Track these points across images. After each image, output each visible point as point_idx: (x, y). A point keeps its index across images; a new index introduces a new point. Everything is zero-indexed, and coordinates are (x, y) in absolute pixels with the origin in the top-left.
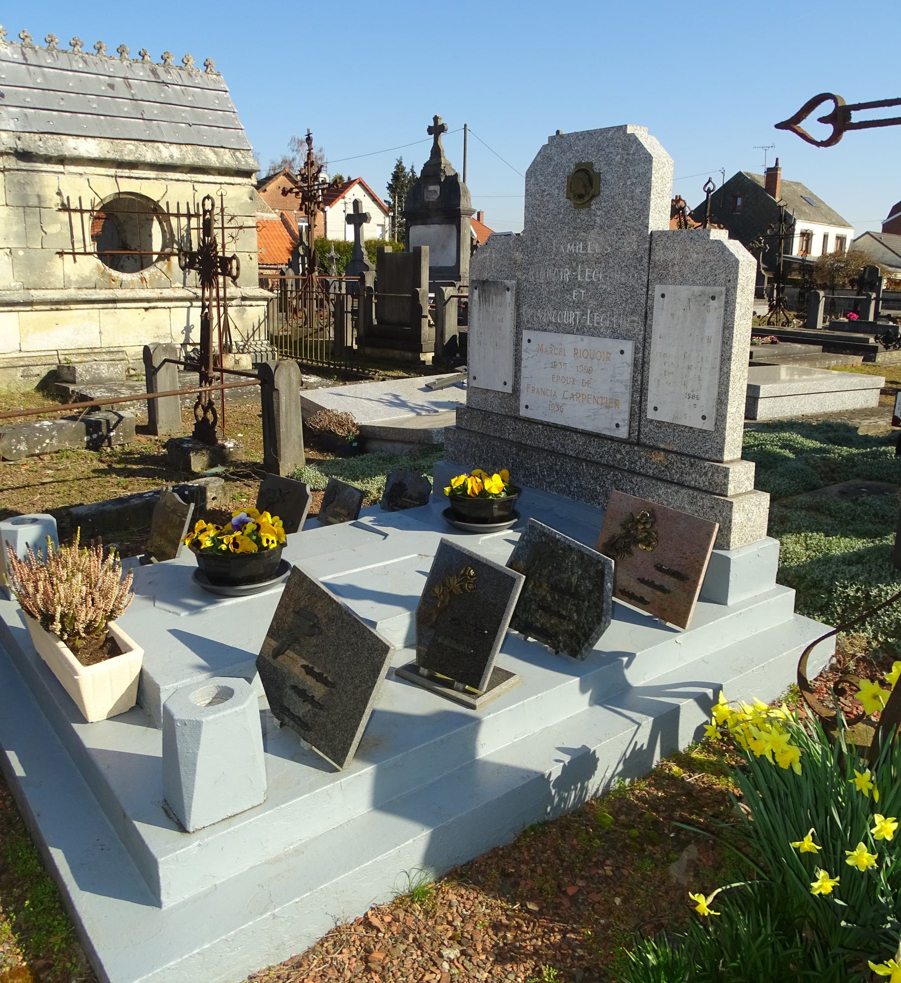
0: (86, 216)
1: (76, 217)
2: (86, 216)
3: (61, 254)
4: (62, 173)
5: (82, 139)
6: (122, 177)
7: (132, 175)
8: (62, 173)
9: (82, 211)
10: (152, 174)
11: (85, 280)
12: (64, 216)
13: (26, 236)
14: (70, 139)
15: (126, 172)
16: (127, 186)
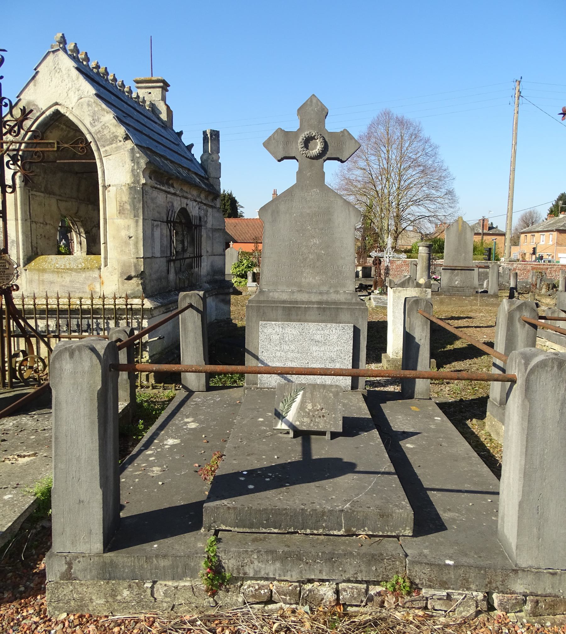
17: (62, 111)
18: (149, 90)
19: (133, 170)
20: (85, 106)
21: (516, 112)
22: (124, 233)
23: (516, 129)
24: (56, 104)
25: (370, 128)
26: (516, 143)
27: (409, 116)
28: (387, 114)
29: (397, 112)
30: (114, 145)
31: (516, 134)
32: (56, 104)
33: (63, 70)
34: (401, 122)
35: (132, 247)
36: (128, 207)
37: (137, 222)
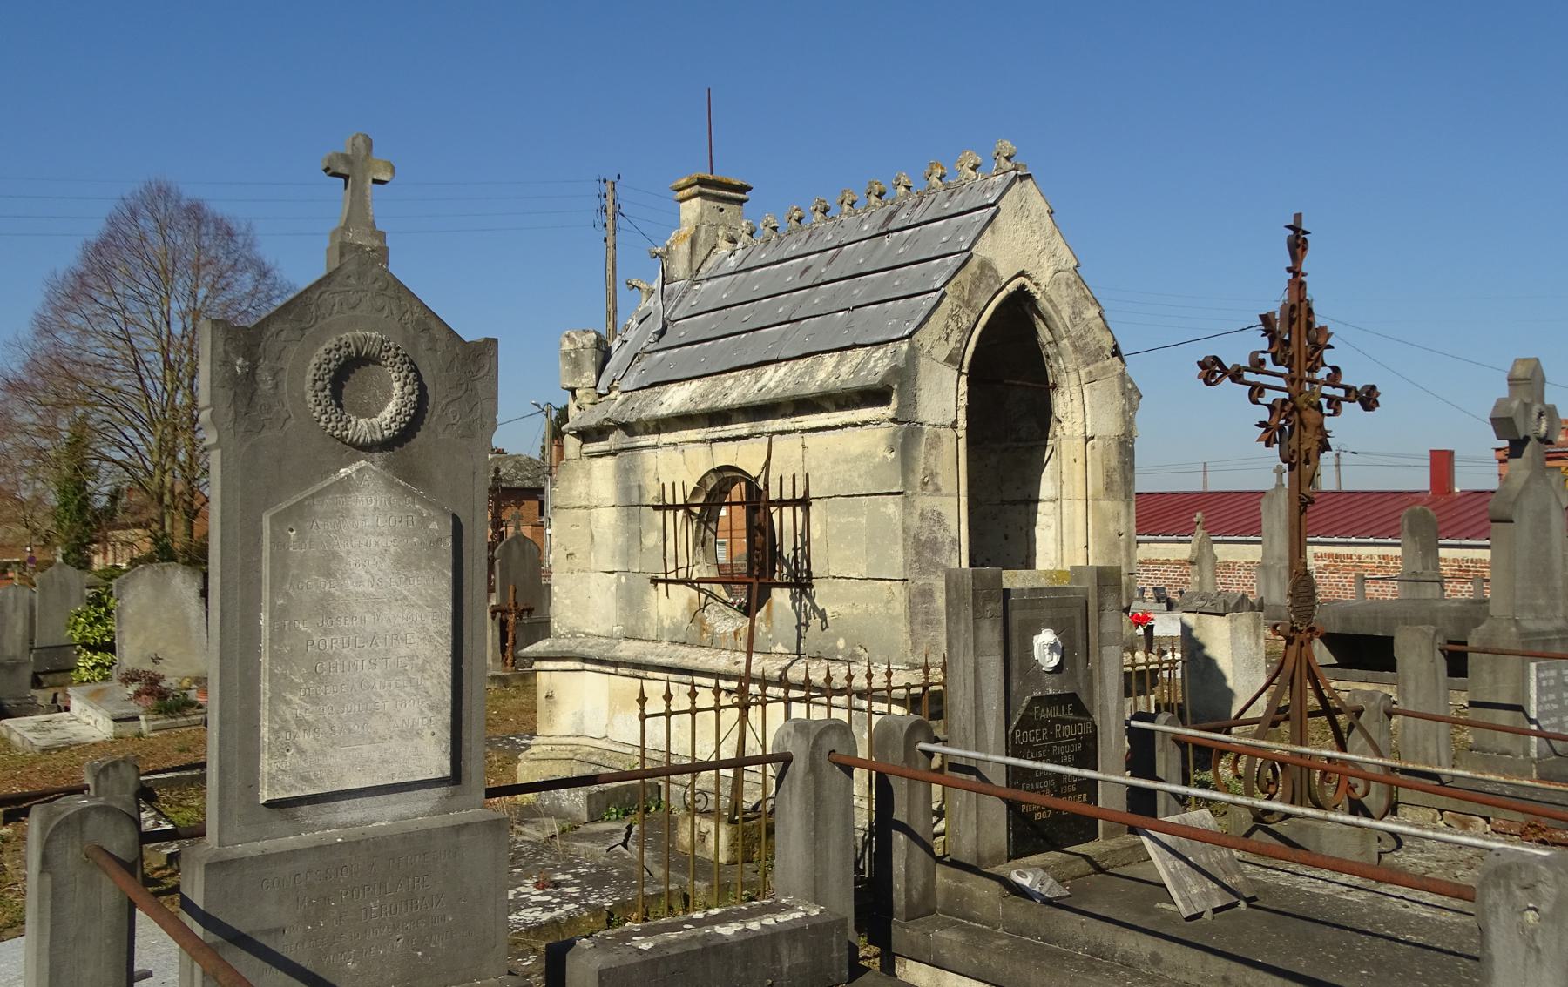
0: (680, 513)
1: (670, 514)
2: (680, 513)
3: (655, 581)
4: (656, 446)
5: (687, 384)
6: (713, 441)
7: (723, 435)
8: (656, 446)
9: (675, 507)
10: (743, 428)
11: (676, 629)
12: (659, 514)
13: (627, 554)
14: (674, 388)
15: (718, 432)
16: (726, 455)
17: (1031, 288)
18: (721, 205)
19: (1124, 411)
20: (1063, 287)
21: (610, 243)
22: (1112, 528)
23: (614, 279)
24: (1022, 274)
25: (112, 221)
26: (615, 311)
27: (220, 205)
28: (164, 192)
29: (190, 192)
30: (1100, 364)
31: (615, 291)
32: (1022, 274)
33: (1033, 212)
34: (195, 214)
35: (1123, 553)
36: (1117, 478)
37: (1128, 505)
